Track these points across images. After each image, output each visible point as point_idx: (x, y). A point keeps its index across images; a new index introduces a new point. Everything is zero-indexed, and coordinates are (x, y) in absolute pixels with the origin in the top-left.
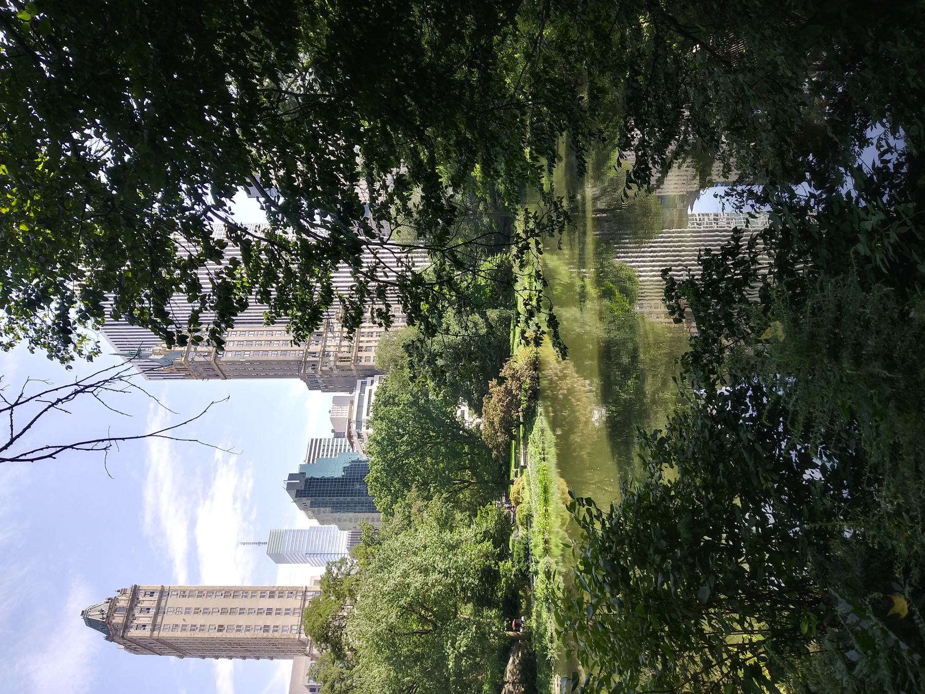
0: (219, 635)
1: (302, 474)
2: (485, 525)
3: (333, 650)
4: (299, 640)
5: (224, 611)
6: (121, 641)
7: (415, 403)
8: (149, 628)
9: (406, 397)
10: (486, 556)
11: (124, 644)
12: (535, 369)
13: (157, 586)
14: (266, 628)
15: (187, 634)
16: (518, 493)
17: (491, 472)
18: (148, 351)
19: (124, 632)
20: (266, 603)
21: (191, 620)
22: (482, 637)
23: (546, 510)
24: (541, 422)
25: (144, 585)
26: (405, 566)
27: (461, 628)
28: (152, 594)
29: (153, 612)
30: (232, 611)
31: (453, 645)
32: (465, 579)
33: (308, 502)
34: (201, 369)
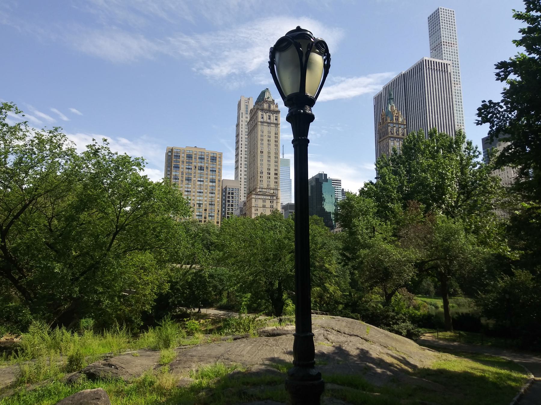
0: (259, 152)
1: (326, 180)
4: (256, 188)
5: (269, 153)
6: (256, 107)
8: (262, 120)
14: (262, 173)
15: (259, 138)
20: (272, 172)
21: (266, 139)
28: (276, 120)
29: (269, 121)
34: (384, 130)
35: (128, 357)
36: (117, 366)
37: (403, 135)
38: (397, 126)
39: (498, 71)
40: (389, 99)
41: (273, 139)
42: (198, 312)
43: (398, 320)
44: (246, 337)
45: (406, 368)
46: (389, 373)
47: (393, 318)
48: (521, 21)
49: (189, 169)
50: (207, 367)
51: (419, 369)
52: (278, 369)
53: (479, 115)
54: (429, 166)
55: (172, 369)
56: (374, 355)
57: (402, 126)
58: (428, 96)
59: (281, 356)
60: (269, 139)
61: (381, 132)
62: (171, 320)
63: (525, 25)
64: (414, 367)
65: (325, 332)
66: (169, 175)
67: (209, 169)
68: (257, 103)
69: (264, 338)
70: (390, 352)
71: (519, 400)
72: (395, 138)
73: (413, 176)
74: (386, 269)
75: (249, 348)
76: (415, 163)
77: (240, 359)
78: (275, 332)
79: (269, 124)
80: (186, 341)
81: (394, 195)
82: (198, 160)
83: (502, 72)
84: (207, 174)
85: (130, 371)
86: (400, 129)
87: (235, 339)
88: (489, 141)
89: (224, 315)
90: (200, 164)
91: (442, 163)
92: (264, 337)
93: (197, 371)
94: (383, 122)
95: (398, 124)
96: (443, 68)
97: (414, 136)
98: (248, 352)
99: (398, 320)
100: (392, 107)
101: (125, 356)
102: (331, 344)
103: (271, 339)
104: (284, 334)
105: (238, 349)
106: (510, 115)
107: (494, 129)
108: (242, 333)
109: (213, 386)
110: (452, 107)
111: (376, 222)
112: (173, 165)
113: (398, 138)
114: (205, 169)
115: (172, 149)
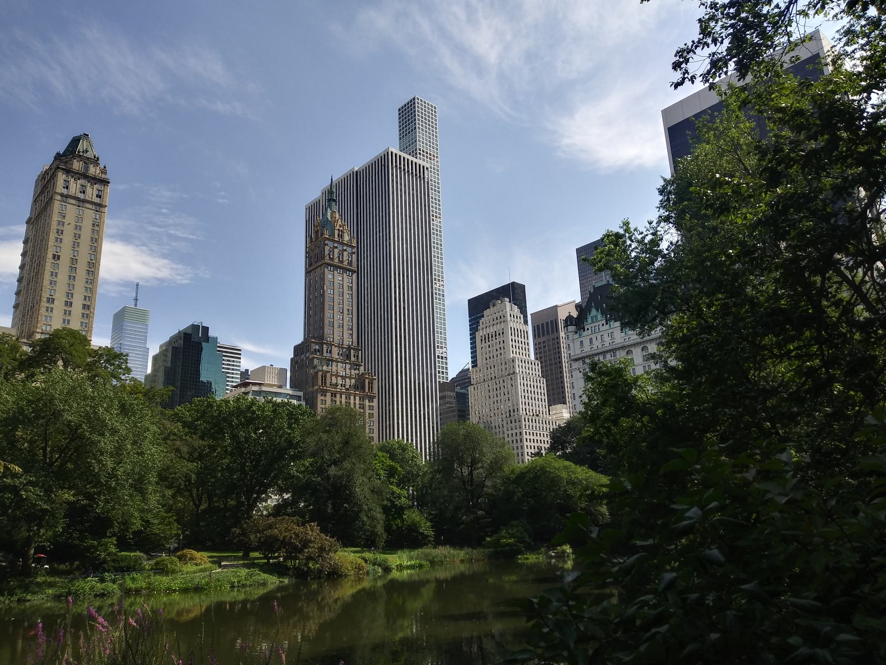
0: (50, 256)
1: (207, 338)
2: (156, 521)
3: (30, 358)
4: (34, 332)
5: (74, 261)
6: (55, 166)
7: (290, 444)
8: (65, 191)
9: (297, 435)
10: (126, 524)
11: (50, 169)
12: (329, 574)
13: (107, 201)
14: (51, 300)
15: (54, 226)
16: (192, 559)
17: (215, 527)
18: (335, 208)
19: (63, 169)
22: (37, 517)
23: (175, 591)
24: (273, 581)
25: (109, 189)
26: (123, 431)
27: (48, 491)
28: (99, 196)
29: (81, 196)
30: (73, 269)
31: (30, 483)
32: (103, 498)
33: (176, 345)
34: (317, 251)
37: (350, 263)
38: (340, 247)
57: (349, 250)
58: (393, 212)
60: (78, 232)
61: (312, 254)
72: (336, 267)
86: (345, 253)
95: (343, 244)
96: (419, 173)
110: (428, 235)
113: (340, 268)
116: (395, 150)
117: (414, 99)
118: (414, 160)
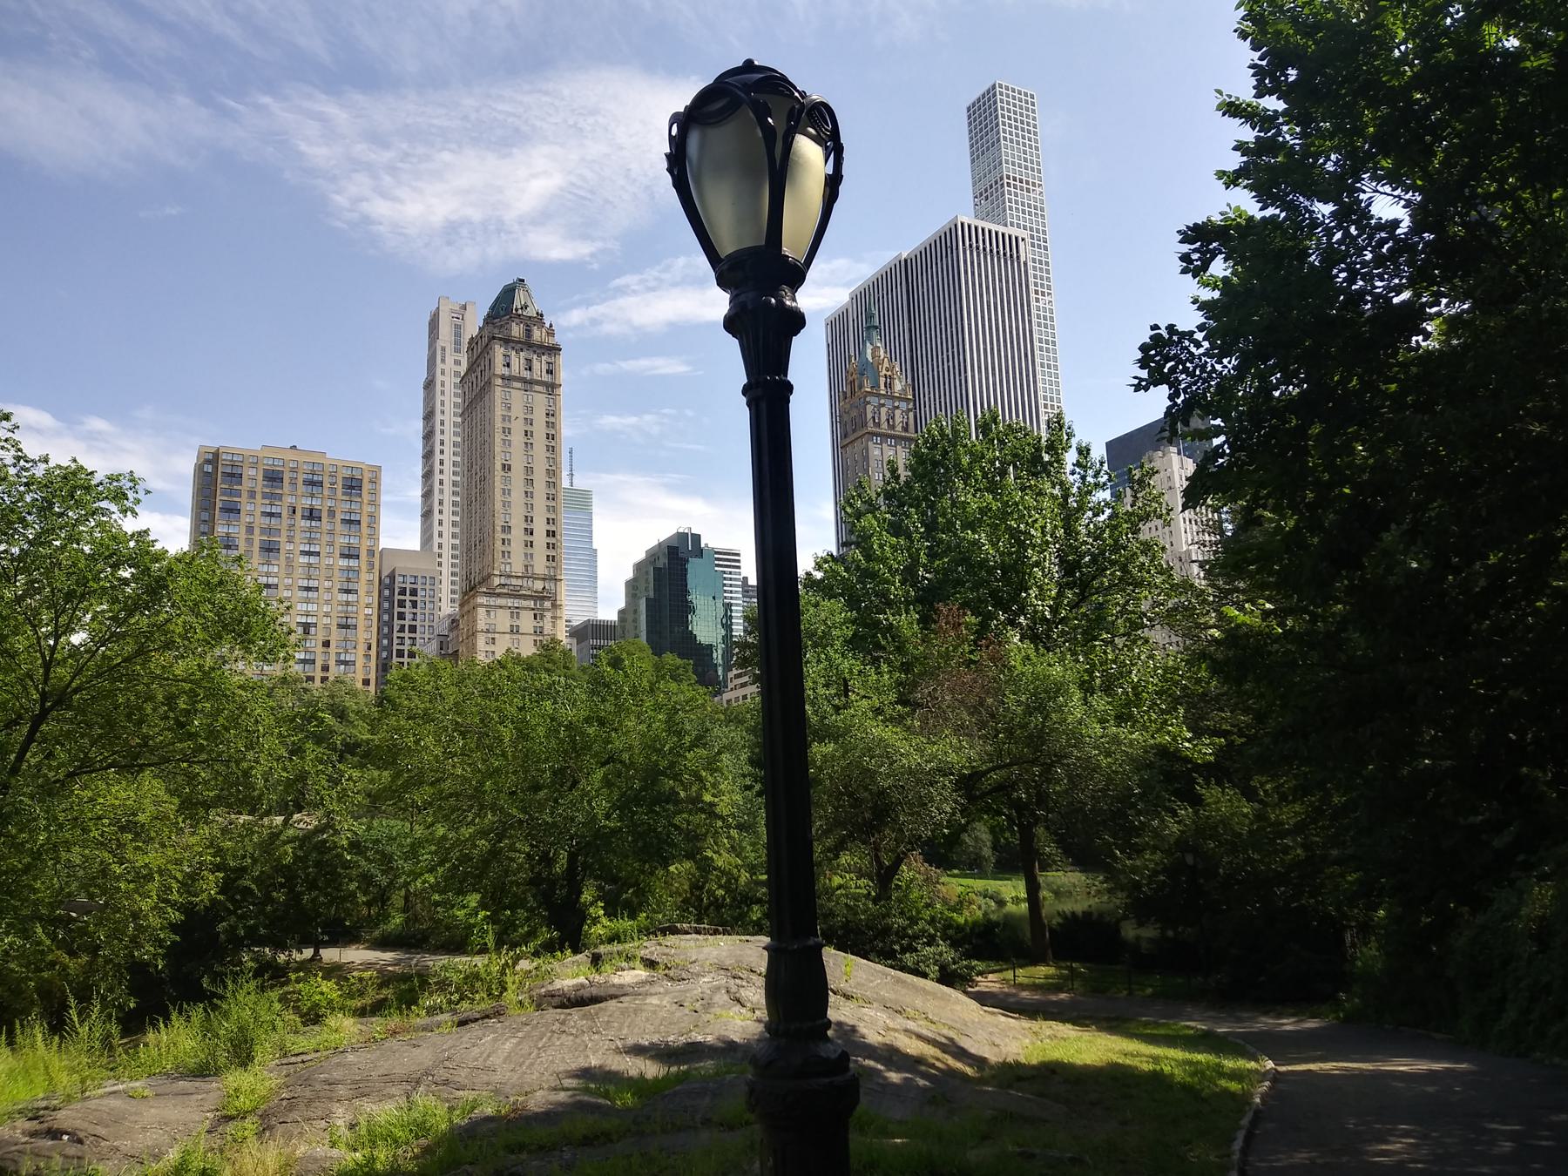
0: (498, 466)
1: (699, 552)
4: (490, 575)
5: (529, 470)
6: (486, 333)
8: (505, 371)
13: (563, 376)
14: (507, 529)
15: (499, 424)
20: (540, 527)
21: (518, 428)
25: (562, 360)
28: (550, 372)
29: (526, 374)
33: (660, 564)
34: (854, 413)
35: (115, 1103)
36: (81, 1135)
37: (906, 429)
38: (889, 404)
39: (1186, 248)
40: (868, 328)
41: (540, 429)
42: (312, 959)
43: (915, 937)
44: (498, 1013)
45: (959, 1065)
46: (921, 1082)
47: (902, 933)
48: (1238, 121)
49: (271, 515)
50: (384, 1112)
51: (992, 1067)
52: (606, 1096)
53: (1143, 363)
54: (983, 511)
55: (270, 1128)
56: (873, 1037)
57: (903, 405)
59: (609, 1062)
60: (529, 428)
61: (846, 418)
62: (255, 977)
63: (1248, 134)
64: (979, 1062)
65: (732, 981)
66: (204, 534)
67: (339, 516)
68: (491, 319)
69: (552, 1014)
70: (911, 1025)
71: (1255, 1122)
72: (885, 436)
73: (941, 541)
74: (882, 793)
75: (508, 1045)
76: (946, 502)
77: (486, 1078)
78: (586, 993)
79: (529, 383)
80: (303, 1042)
81: (896, 590)
82: (301, 488)
83: (1195, 251)
84: (331, 533)
85: (126, 1145)
87: (462, 1023)
88: (1167, 434)
89: (397, 963)
90: (307, 502)
91: (1017, 504)
92: (551, 1010)
93: (352, 1126)
94: (853, 393)
95: (893, 398)
97: (941, 429)
98: (507, 1059)
99: (915, 937)
100: (875, 350)
101: (105, 1101)
102: (750, 1014)
103: (575, 1013)
104: (612, 997)
105: (476, 1050)
106: (1218, 367)
107: (1179, 401)
108: (480, 1005)
109: (411, 1167)
111: (849, 665)
112: (219, 505)
113: (892, 437)
114: (324, 515)
115: (216, 455)
116: (967, 218)
117: (994, 87)
118: (1001, 229)
